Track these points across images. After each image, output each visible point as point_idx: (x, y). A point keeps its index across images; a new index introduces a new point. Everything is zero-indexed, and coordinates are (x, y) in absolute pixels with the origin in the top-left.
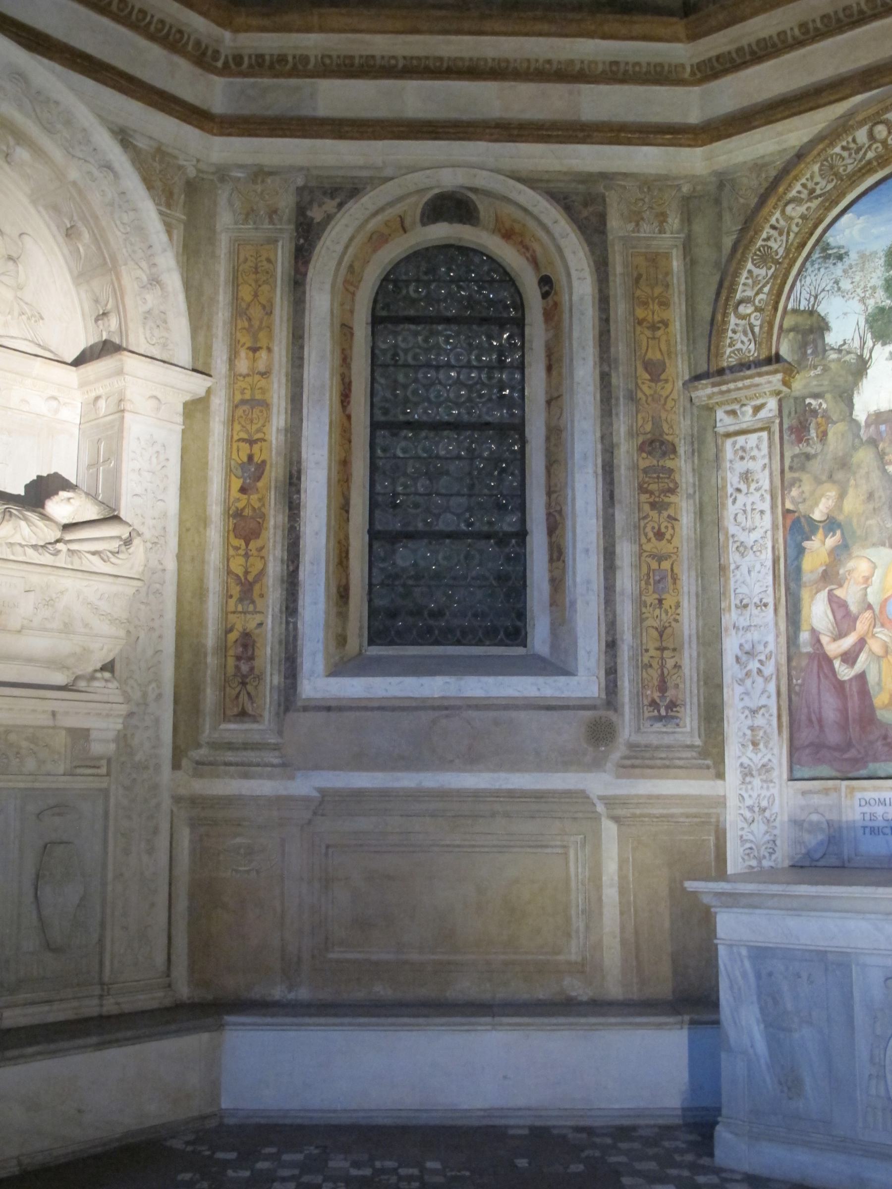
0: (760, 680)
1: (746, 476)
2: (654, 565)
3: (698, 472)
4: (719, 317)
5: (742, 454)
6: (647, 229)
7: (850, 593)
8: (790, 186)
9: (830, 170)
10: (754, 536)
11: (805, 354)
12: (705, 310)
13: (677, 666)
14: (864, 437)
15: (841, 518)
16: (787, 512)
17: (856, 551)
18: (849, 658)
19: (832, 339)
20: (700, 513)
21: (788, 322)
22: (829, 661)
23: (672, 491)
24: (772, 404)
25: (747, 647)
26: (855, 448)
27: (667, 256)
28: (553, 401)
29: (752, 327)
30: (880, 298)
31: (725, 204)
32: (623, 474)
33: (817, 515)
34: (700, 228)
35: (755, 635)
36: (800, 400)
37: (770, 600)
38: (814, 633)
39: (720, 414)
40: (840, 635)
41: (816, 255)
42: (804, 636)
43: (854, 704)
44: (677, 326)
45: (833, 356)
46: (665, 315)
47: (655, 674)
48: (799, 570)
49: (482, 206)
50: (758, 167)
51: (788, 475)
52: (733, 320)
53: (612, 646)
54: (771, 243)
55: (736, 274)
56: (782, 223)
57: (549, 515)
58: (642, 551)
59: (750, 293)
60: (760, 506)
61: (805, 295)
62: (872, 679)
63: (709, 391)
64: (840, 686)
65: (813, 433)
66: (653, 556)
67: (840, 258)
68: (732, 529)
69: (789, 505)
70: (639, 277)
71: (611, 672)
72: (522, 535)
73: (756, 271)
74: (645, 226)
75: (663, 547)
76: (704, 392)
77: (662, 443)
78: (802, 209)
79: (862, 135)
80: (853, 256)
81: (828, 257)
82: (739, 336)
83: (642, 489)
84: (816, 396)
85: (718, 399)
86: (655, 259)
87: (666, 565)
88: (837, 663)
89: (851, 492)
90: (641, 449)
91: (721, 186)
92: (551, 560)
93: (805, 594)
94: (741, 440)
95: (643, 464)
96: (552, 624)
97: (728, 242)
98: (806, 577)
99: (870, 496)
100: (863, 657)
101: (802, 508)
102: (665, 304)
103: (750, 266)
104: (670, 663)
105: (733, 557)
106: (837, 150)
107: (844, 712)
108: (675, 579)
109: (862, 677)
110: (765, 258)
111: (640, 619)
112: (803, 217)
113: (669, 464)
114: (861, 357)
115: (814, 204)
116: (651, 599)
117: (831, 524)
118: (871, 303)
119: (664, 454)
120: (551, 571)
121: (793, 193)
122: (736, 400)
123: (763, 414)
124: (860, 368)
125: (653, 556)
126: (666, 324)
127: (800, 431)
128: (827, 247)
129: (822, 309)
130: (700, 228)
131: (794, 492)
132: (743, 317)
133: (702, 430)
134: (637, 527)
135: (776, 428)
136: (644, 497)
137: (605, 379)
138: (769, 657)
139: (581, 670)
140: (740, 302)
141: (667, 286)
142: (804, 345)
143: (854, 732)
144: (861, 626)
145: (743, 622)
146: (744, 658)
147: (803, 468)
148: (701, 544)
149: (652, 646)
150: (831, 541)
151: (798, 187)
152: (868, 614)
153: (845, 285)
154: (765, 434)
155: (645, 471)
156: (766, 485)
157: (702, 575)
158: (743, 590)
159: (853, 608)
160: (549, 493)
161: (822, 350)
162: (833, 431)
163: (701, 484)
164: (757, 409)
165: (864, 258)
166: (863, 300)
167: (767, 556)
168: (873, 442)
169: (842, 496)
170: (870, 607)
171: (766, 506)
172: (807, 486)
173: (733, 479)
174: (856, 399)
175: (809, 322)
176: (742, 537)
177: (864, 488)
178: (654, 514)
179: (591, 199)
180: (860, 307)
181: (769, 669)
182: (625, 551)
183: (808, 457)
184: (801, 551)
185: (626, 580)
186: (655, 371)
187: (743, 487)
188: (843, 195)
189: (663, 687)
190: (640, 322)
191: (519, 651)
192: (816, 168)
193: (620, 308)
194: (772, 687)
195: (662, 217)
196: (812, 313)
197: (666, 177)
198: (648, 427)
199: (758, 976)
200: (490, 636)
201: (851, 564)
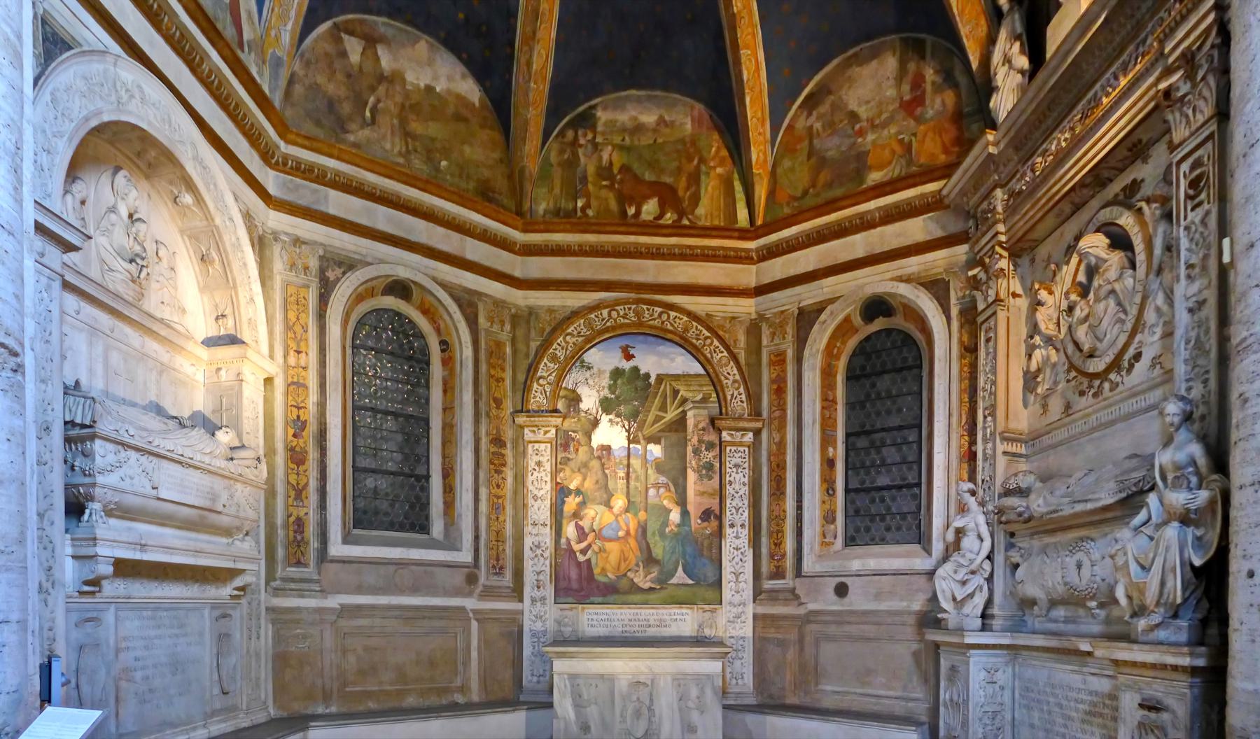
0: (542, 559)
1: (539, 464)
2: (495, 500)
3: (515, 457)
4: (529, 382)
5: (537, 452)
6: (496, 328)
7: (585, 524)
8: (568, 327)
9: (589, 325)
10: (542, 492)
11: (570, 411)
12: (521, 377)
13: (504, 550)
14: (596, 454)
15: (583, 490)
16: (557, 484)
17: (589, 505)
18: (584, 552)
19: (583, 406)
20: (516, 477)
21: (562, 393)
22: (575, 553)
23: (504, 465)
24: (553, 431)
25: (536, 543)
26: (591, 459)
27: (505, 344)
28: (448, 409)
29: (545, 392)
30: (606, 393)
31: (532, 324)
32: (483, 453)
33: (572, 487)
34: (520, 332)
35: (540, 538)
36: (566, 432)
37: (548, 523)
38: (568, 540)
39: (526, 431)
40: (580, 541)
41: (577, 364)
42: (563, 541)
43: (585, 572)
44: (508, 382)
45: (583, 414)
46: (503, 375)
47: (494, 553)
48: (562, 510)
49: (416, 293)
50: (551, 310)
51: (559, 466)
52: (535, 385)
53: (477, 538)
54: (557, 352)
55: (539, 363)
56: (563, 344)
57: (443, 469)
58: (490, 493)
59: (545, 374)
60: (545, 479)
61: (571, 382)
62: (593, 561)
63: (525, 419)
64: (579, 564)
65: (572, 449)
66: (495, 496)
67: (589, 368)
68: (531, 488)
69: (558, 480)
70: (492, 352)
71: (476, 550)
72: (427, 477)
73: (549, 364)
74: (495, 326)
75: (499, 492)
76: (521, 419)
77: (500, 440)
78: (574, 340)
79: (605, 312)
80: (595, 369)
81: (583, 366)
82: (538, 394)
83: (491, 463)
84: (574, 432)
85: (528, 423)
86: (499, 345)
87: (500, 501)
88: (578, 554)
89: (588, 479)
90: (491, 442)
91: (530, 314)
92: (445, 492)
93: (565, 522)
94: (537, 446)
95: (492, 450)
96: (446, 524)
97: (534, 345)
98: (565, 514)
99: (597, 482)
100: (590, 552)
101: (565, 483)
102: (503, 370)
103: (545, 360)
104: (501, 548)
105: (530, 501)
106: (593, 316)
107: (580, 576)
108: (504, 509)
109: (589, 561)
110: (554, 359)
111: (489, 526)
112: (574, 343)
113: (503, 452)
114: (596, 418)
115: (580, 339)
116: (493, 517)
117: (578, 492)
118: (602, 393)
119: (501, 447)
120: (444, 498)
121: (570, 331)
122: (536, 426)
123: (548, 435)
124: (595, 423)
125: (495, 496)
126: (503, 380)
127: (566, 447)
128: (583, 362)
129: (579, 391)
130: (520, 332)
131: (562, 474)
132: (541, 386)
133: (518, 437)
134: (489, 481)
135: (554, 443)
136: (492, 466)
137: (476, 402)
138: (547, 549)
139: (464, 549)
140: (541, 377)
141: (504, 360)
142: (569, 407)
143: (585, 584)
144: (590, 538)
145: (534, 531)
146: (534, 548)
147: (566, 464)
148: (515, 492)
149: (494, 539)
150: (578, 500)
151: (572, 328)
152: (593, 534)
153: (591, 382)
154: (549, 445)
155: (493, 453)
156: (549, 470)
157: (515, 508)
158: (535, 517)
159: (587, 530)
160: (444, 457)
161: (578, 411)
162: (581, 449)
163: (516, 464)
164: (546, 432)
165: (600, 372)
166: (598, 391)
167: (548, 503)
168: (600, 458)
169: (584, 479)
170: (594, 531)
171: (548, 479)
172: (568, 472)
173: (532, 464)
174: (593, 437)
175: (572, 396)
176: (536, 492)
177: (595, 478)
178: (496, 475)
179: (473, 305)
180: (596, 395)
181: (547, 554)
182: (483, 492)
183: (569, 459)
184: (564, 502)
185: (483, 507)
186: (498, 403)
187: (537, 468)
188: (594, 338)
189: (498, 559)
190: (492, 376)
191: (424, 537)
192: (582, 321)
193: (483, 367)
194: (548, 562)
195: (502, 323)
196: (574, 391)
197: (504, 302)
198: (495, 432)
199: (572, 686)
200: (412, 528)
201: (586, 511)
